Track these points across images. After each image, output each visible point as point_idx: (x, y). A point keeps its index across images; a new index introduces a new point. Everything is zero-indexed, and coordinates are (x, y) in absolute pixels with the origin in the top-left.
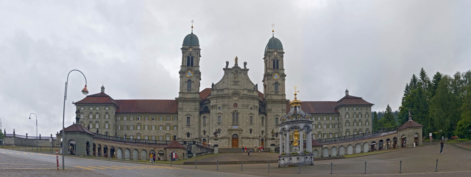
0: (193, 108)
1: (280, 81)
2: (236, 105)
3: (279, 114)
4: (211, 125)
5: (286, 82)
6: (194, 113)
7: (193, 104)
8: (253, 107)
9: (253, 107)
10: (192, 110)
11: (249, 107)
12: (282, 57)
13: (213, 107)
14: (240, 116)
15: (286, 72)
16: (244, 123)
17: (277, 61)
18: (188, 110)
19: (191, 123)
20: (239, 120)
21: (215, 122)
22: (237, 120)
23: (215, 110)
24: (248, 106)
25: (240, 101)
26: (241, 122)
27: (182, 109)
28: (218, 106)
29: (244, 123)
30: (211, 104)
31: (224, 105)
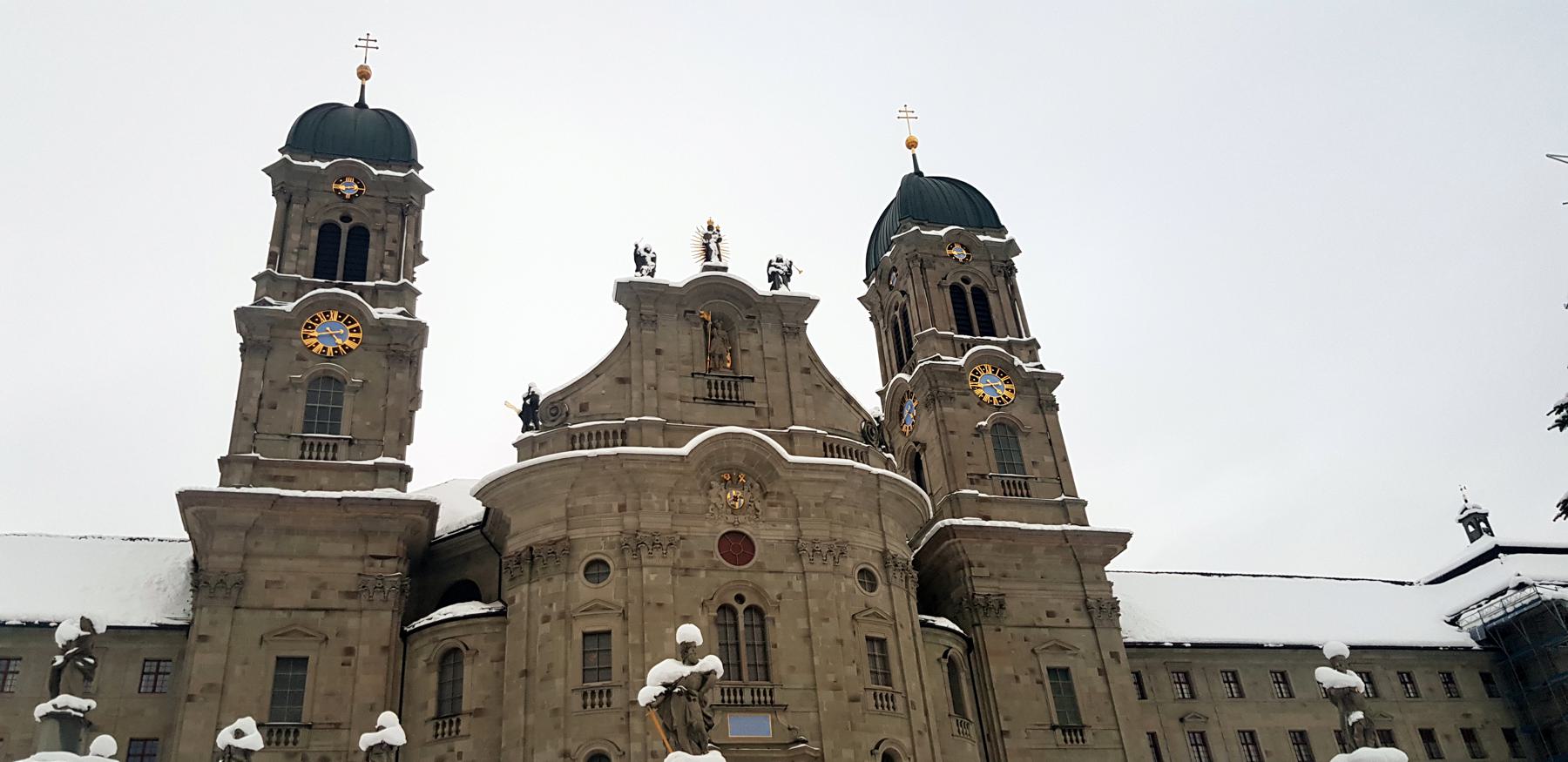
0: (350, 584)
1: (1022, 412)
2: (737, 547)
3: (1067, 637)
4: (518, 719)
5: (1067, 419)
6: (352, 622)
7: (347, 549)
8: (875, 567)
9: (875, 567)
10: (332, 600)
11: (849, 564)
12: (1010, 271)
13: (531, 557)
14: (784, 633)
15: (1049, 361)
16: (826, 696)
17: (979, 294)
18: (301, 597)
19: (311, 710)
20: (779, 669)
21: (564, 683)
22: (764, 668)
23: (558, 583)
24: (839, 551)
25: (774, 513)
26: (800, 680)
27: (240, 585)
28: (584, 555)
29: (826, 696)
30: (514, 545)
31: (635, 545)
